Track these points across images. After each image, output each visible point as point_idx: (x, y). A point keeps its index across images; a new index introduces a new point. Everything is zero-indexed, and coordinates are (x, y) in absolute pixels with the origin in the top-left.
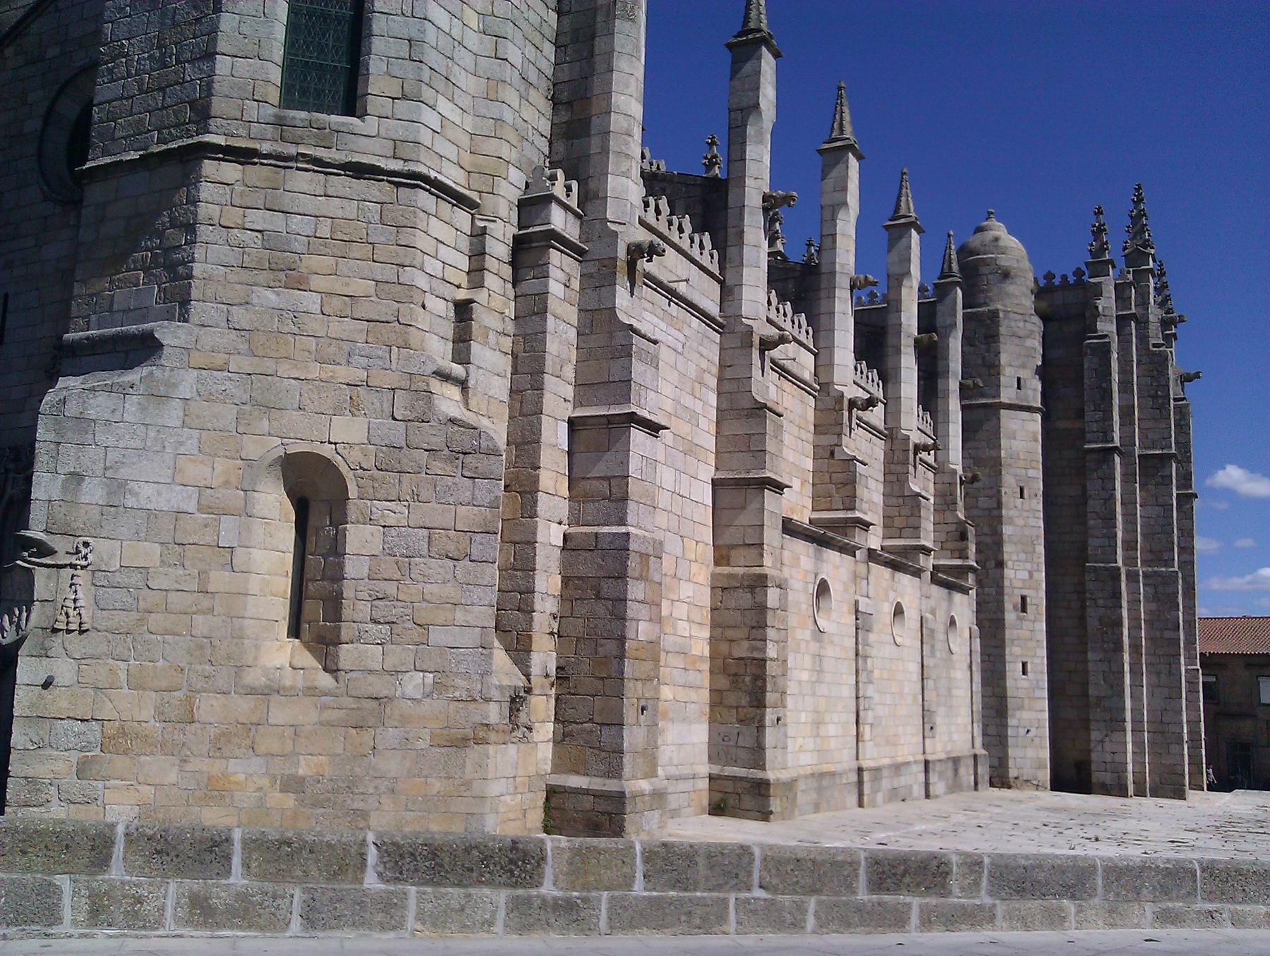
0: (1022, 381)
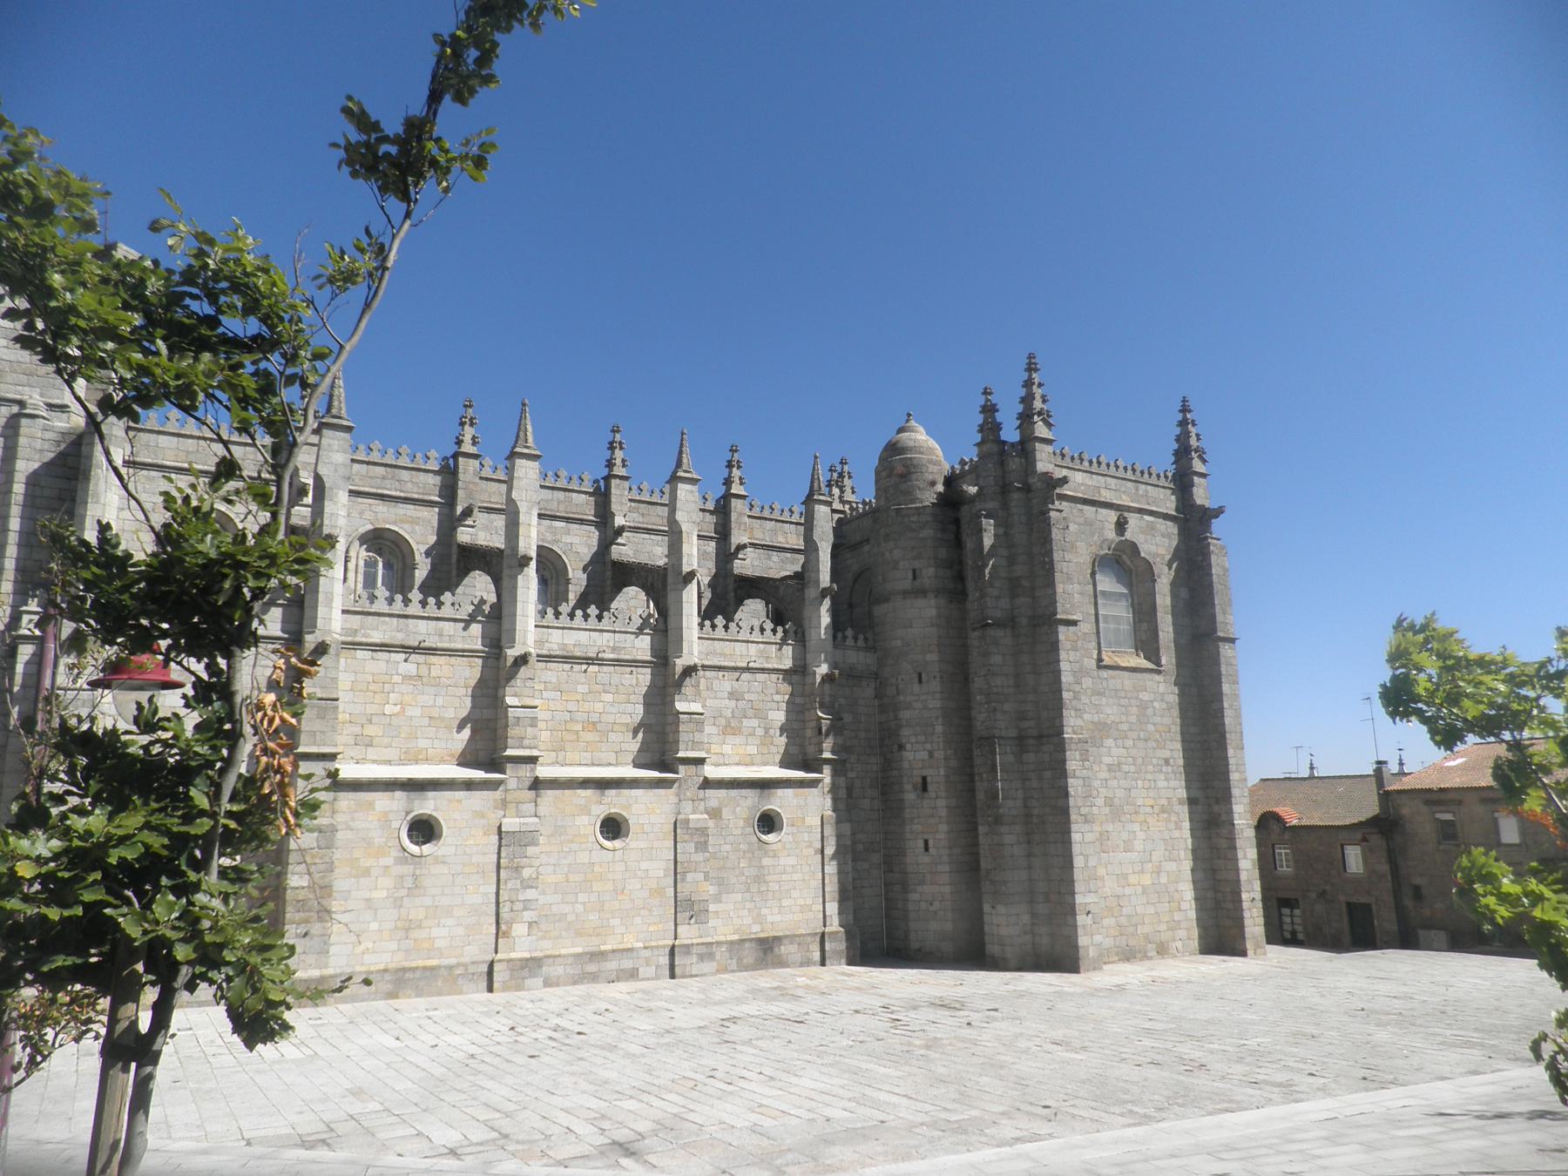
0: (917, 572)
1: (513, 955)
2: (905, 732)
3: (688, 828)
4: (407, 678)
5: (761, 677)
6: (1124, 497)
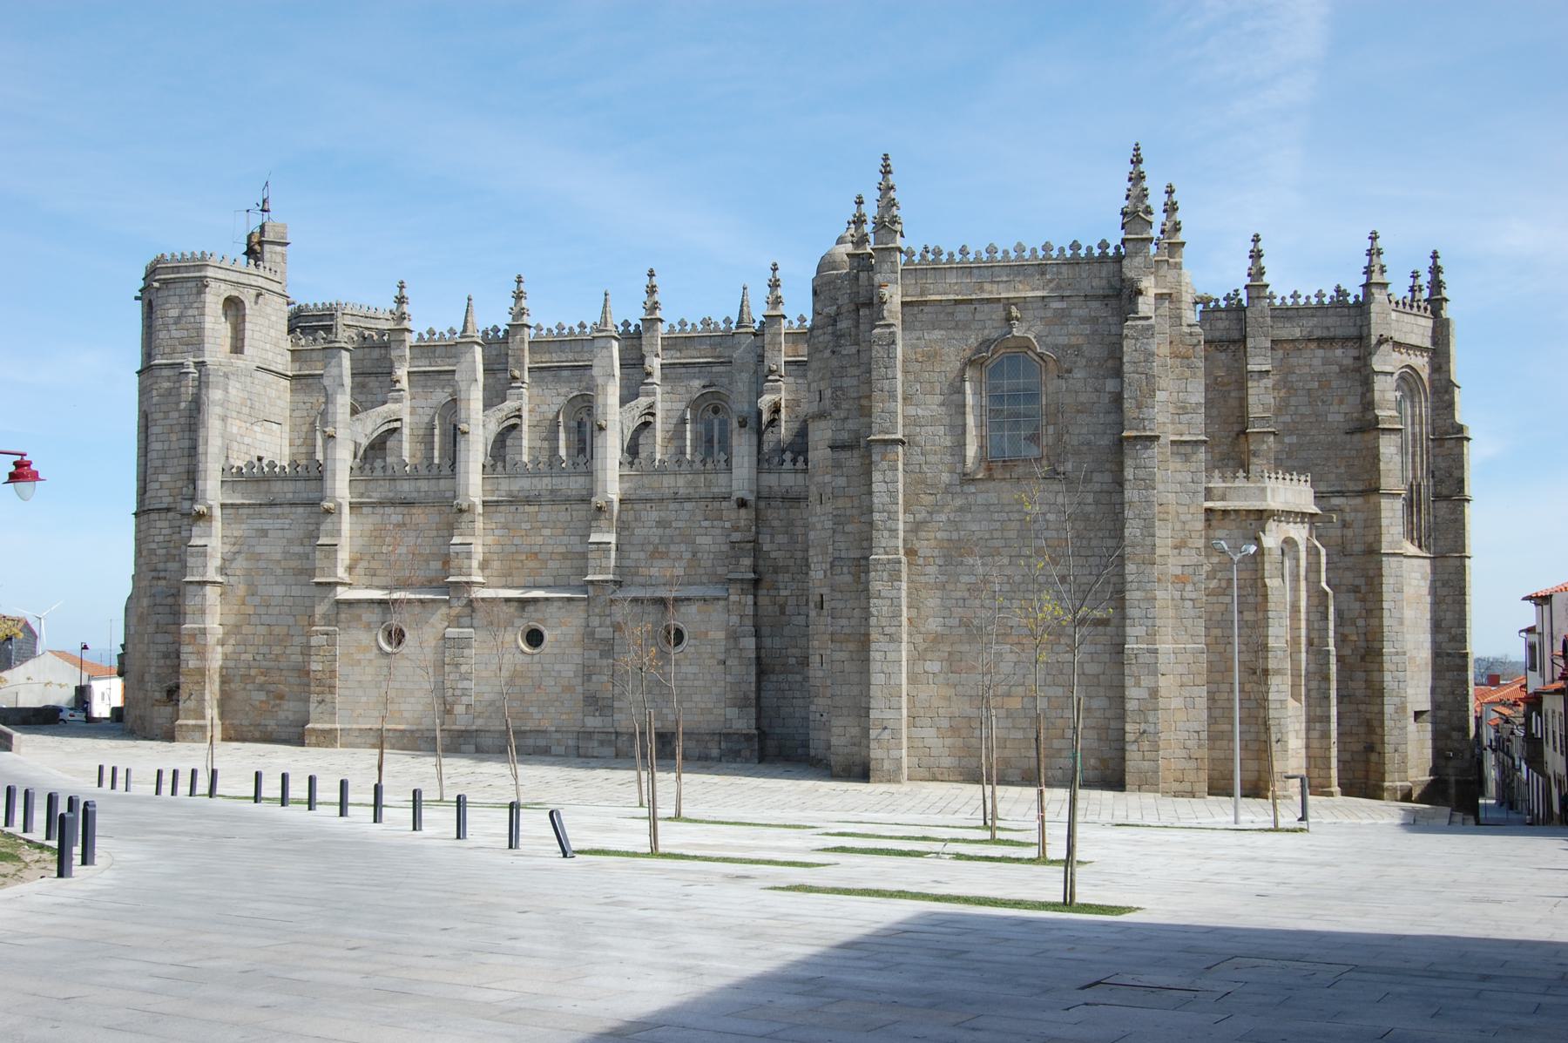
1: (454, 727)
2: (811, 553)
3: (594, 639)
4: (398, 525)
5: (688, 506)
6: (1021, 287)
